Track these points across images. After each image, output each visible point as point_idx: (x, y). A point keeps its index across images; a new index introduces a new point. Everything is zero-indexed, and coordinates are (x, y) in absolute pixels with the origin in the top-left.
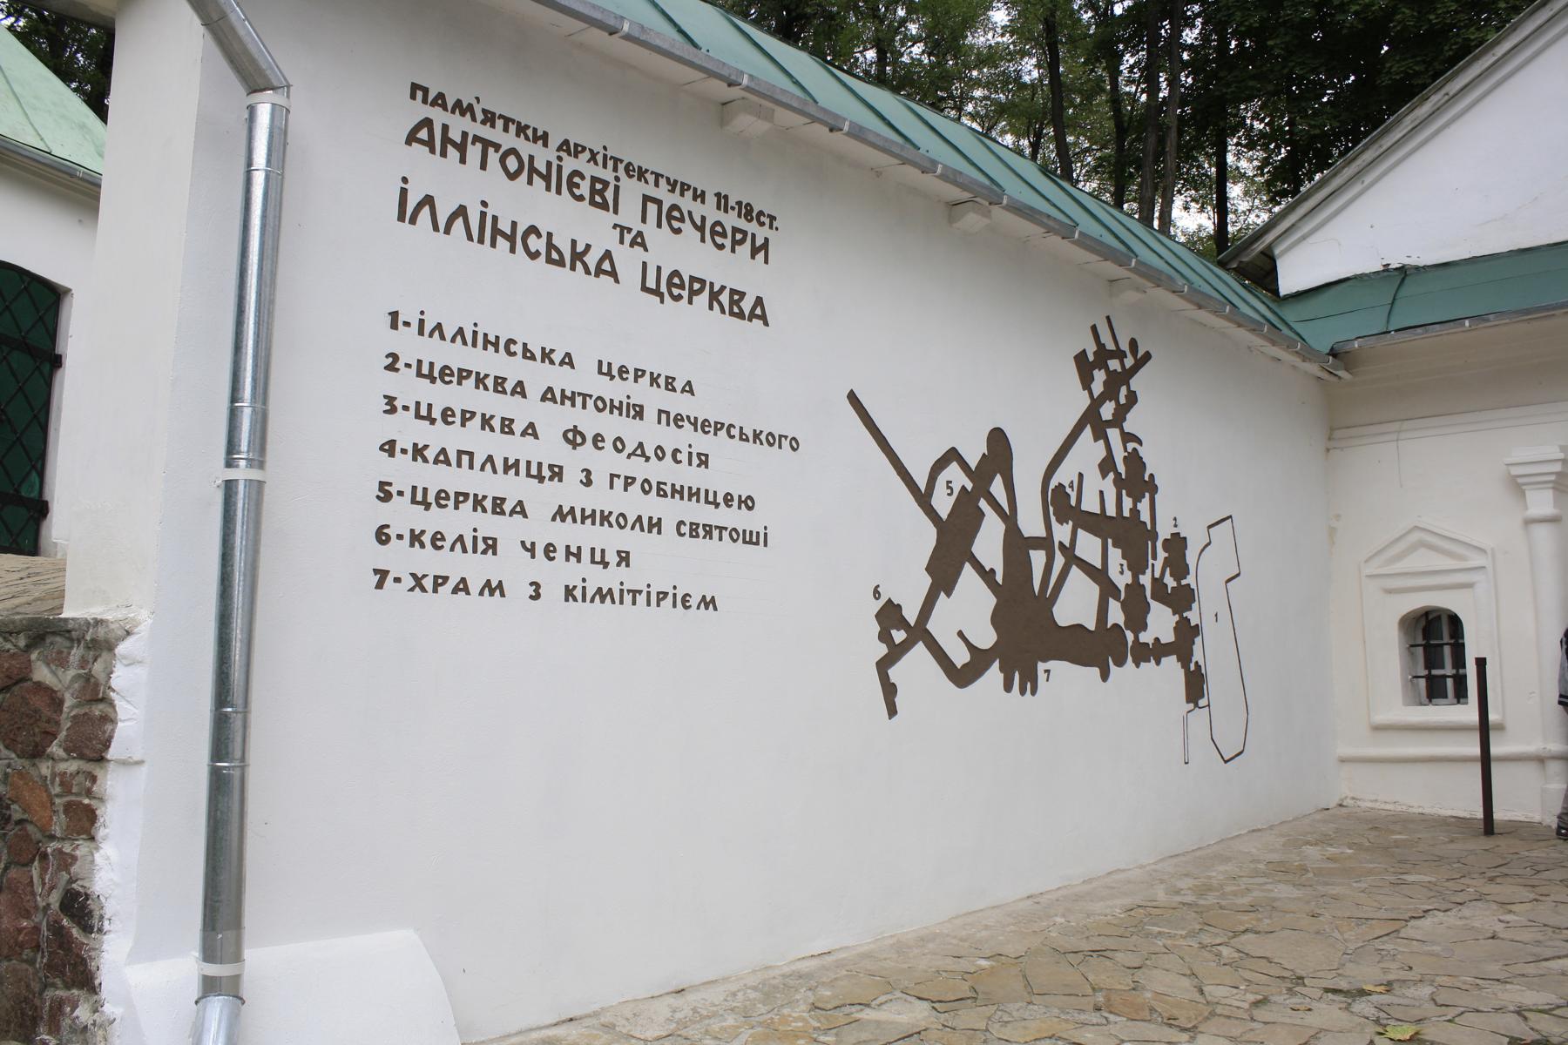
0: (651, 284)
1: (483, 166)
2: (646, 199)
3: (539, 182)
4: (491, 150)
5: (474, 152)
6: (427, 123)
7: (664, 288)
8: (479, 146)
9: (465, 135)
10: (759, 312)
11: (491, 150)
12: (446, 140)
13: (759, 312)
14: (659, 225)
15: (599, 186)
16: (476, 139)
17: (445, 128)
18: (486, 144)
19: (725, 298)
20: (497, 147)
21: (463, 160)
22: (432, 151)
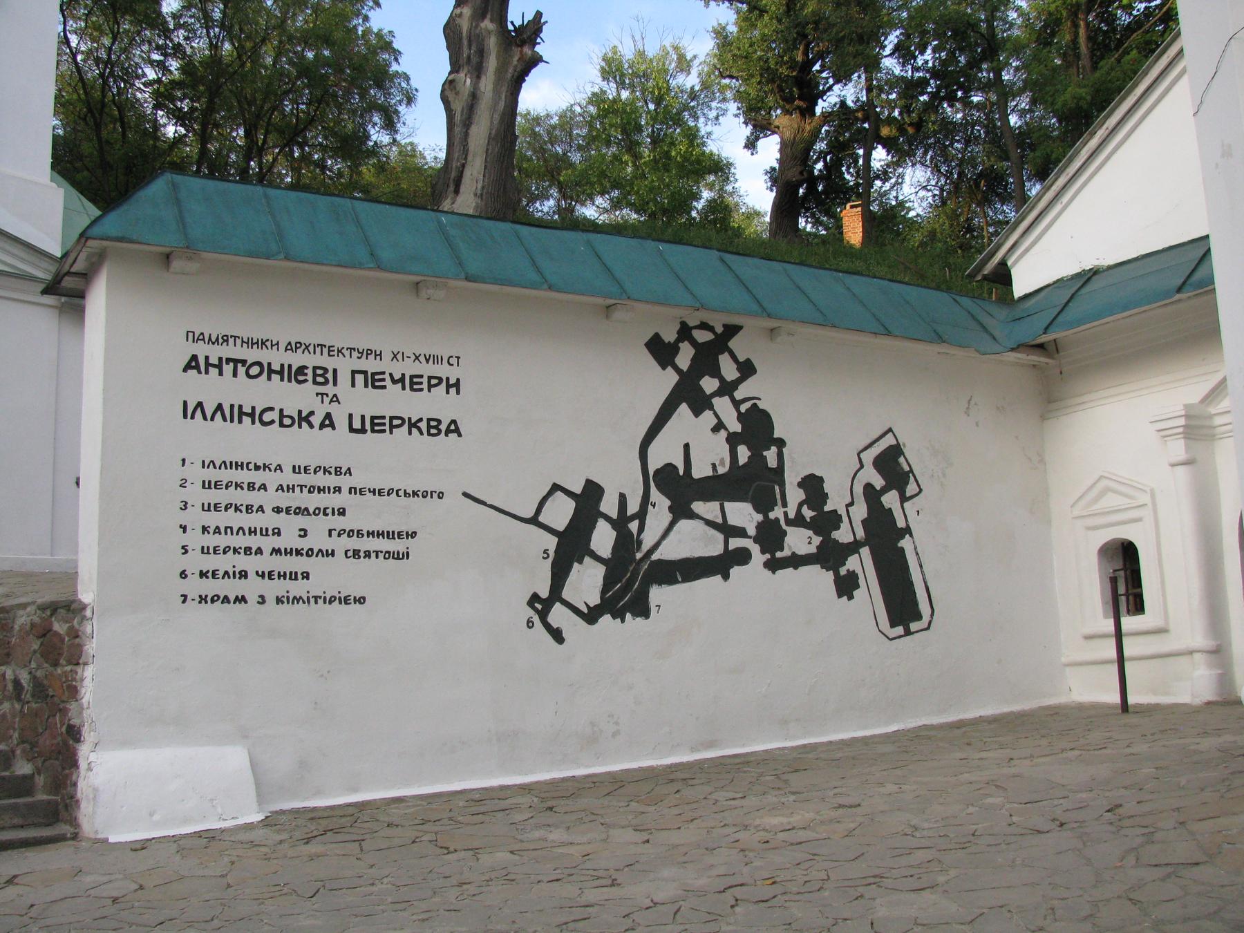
0: (357, 425)
1: (235, 375)
2: (354, 372)
3: (275, 377)
4: (239, 365)
5: (228, 369)
6: (194, 358)
7: (368, 426)
8: (232, 364)
9: (220, 359)
10: (454, 428)
11: (239, 365)
12: (208, 364)
13: (454, 428)
14: (366, 386)
15: (319, 372)
16: (229, 360)
17: (207, 358)
18: (236, 361)
19: (423, 425)
20: (244, 362)
21: (221, 374)
22: (200, 372)
